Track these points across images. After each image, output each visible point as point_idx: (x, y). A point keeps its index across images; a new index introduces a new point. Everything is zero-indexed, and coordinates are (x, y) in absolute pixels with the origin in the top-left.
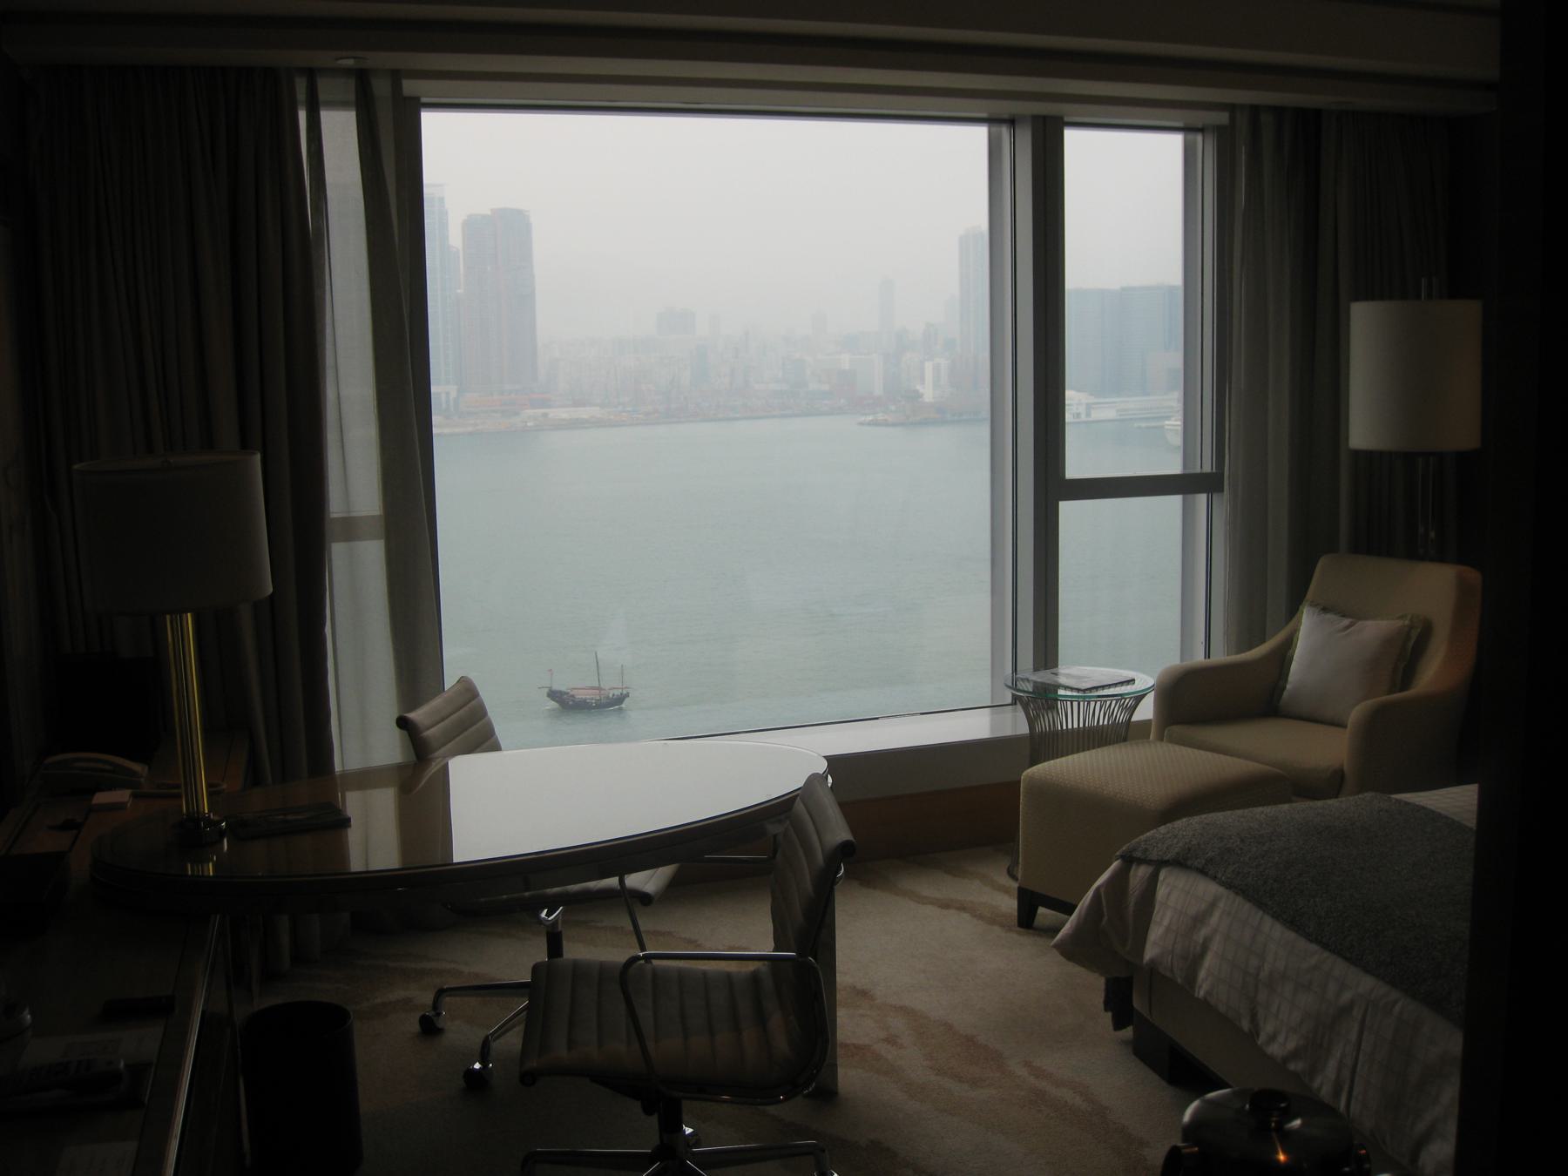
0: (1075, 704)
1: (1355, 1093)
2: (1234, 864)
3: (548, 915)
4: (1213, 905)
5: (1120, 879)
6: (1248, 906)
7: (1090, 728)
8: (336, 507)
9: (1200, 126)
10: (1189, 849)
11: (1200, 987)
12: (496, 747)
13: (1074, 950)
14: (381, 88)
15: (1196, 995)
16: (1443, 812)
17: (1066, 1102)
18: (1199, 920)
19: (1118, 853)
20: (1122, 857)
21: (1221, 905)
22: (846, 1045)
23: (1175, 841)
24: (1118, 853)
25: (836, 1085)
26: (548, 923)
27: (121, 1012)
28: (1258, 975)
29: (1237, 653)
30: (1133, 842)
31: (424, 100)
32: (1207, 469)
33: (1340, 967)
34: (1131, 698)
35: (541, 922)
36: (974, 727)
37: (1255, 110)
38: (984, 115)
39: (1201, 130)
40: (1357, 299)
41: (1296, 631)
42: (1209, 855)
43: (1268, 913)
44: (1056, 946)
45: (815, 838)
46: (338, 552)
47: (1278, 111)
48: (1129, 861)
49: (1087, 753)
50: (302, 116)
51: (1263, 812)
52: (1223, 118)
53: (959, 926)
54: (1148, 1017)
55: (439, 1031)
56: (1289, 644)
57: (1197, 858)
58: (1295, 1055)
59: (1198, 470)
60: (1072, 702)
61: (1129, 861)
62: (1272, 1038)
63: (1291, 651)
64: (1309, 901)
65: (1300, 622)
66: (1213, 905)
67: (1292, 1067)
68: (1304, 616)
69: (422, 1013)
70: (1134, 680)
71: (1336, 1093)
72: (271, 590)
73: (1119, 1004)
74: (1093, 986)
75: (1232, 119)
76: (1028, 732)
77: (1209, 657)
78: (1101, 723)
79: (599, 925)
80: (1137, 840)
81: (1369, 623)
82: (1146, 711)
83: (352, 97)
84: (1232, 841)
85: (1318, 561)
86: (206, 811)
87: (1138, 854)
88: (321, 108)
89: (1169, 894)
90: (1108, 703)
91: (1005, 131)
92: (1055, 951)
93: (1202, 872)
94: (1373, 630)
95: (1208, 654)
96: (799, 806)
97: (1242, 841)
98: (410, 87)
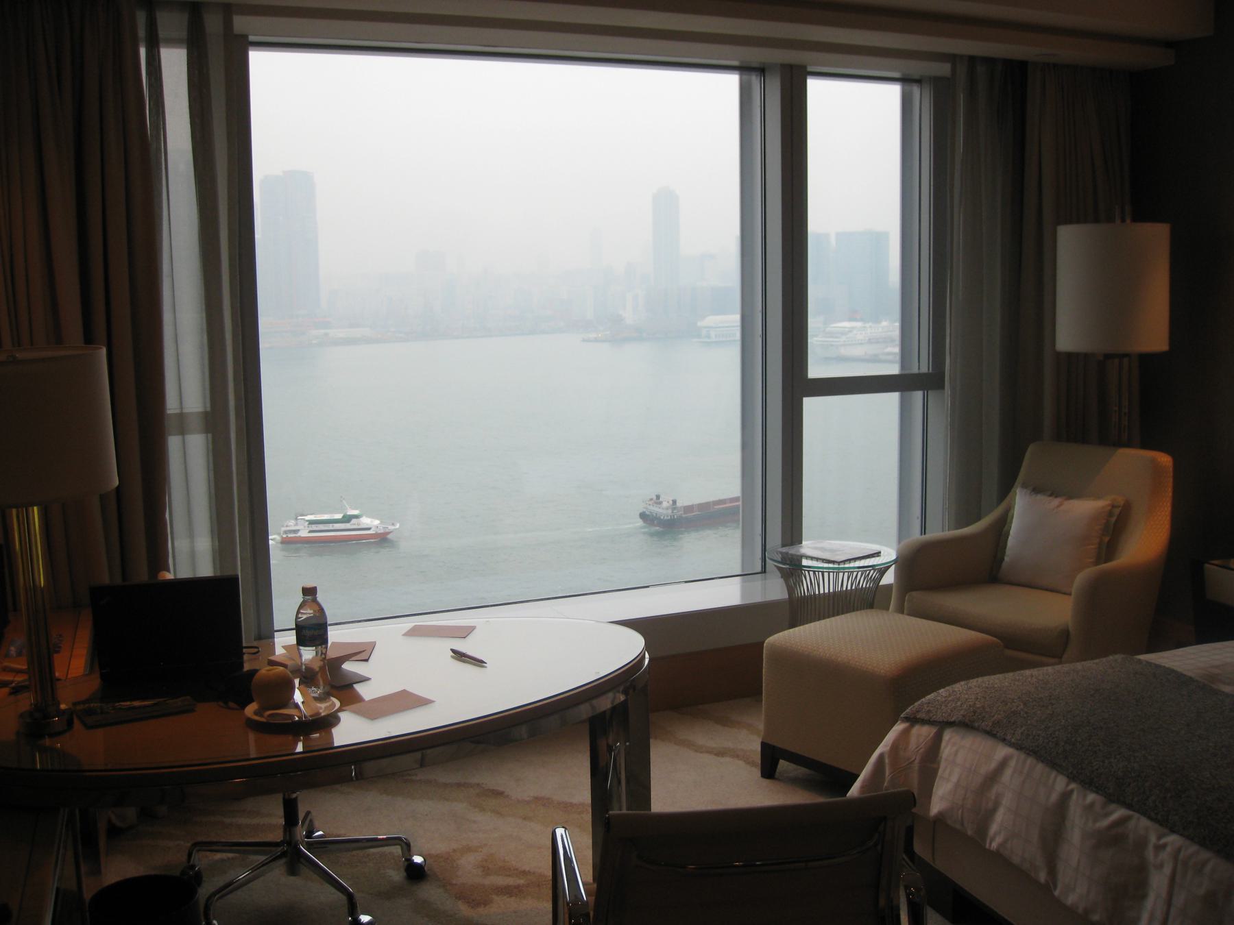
2: (1022, 727)
6: (1040, 766)
7: (834, 592)
8: (172, 405)
9: (917, 77)
10: (975, 712)
11: (992, 840)
14: (213, 23)
15: (987, 846)
19: (902, 716)
21: (1012, 763)
23: (959, 703)
29: (957, 529)
30: (916, 704)
31: (252, 38)
32: (924, 370)
36: (727, 594)
37: (972, 60)
38: (736, 63)
39: (918, 81)
41: (1009, 509)
42: (995, 717)
43: (1062, 773)
46: (173, 443)
47: (989, 61)
50: (143, 52)
51: (1032, 676)
52: (944, 69)
54: (932, 863)
57: (983, 721)
59: (915, 370)
60: (823, 573)
63: (1006, 527)
64: (1103, 762)
66: (1003, 764)
68: (1018, 498)
70: (880, 552)
76: (786, 596)
77: (925, 534)
78: (849, 588)
79: (414, 778)
80: (919, 702)
82: (889, 578)
83: (184, 34)
85: (1028, 447)
88: (161, 44)
89: (956, 753)
90: (855, 574)
91: (755, 80)
93: (990, 734)
94: (1084, 508)
95: (924, 530)
97: (1025, 704)
98: (241, 23)
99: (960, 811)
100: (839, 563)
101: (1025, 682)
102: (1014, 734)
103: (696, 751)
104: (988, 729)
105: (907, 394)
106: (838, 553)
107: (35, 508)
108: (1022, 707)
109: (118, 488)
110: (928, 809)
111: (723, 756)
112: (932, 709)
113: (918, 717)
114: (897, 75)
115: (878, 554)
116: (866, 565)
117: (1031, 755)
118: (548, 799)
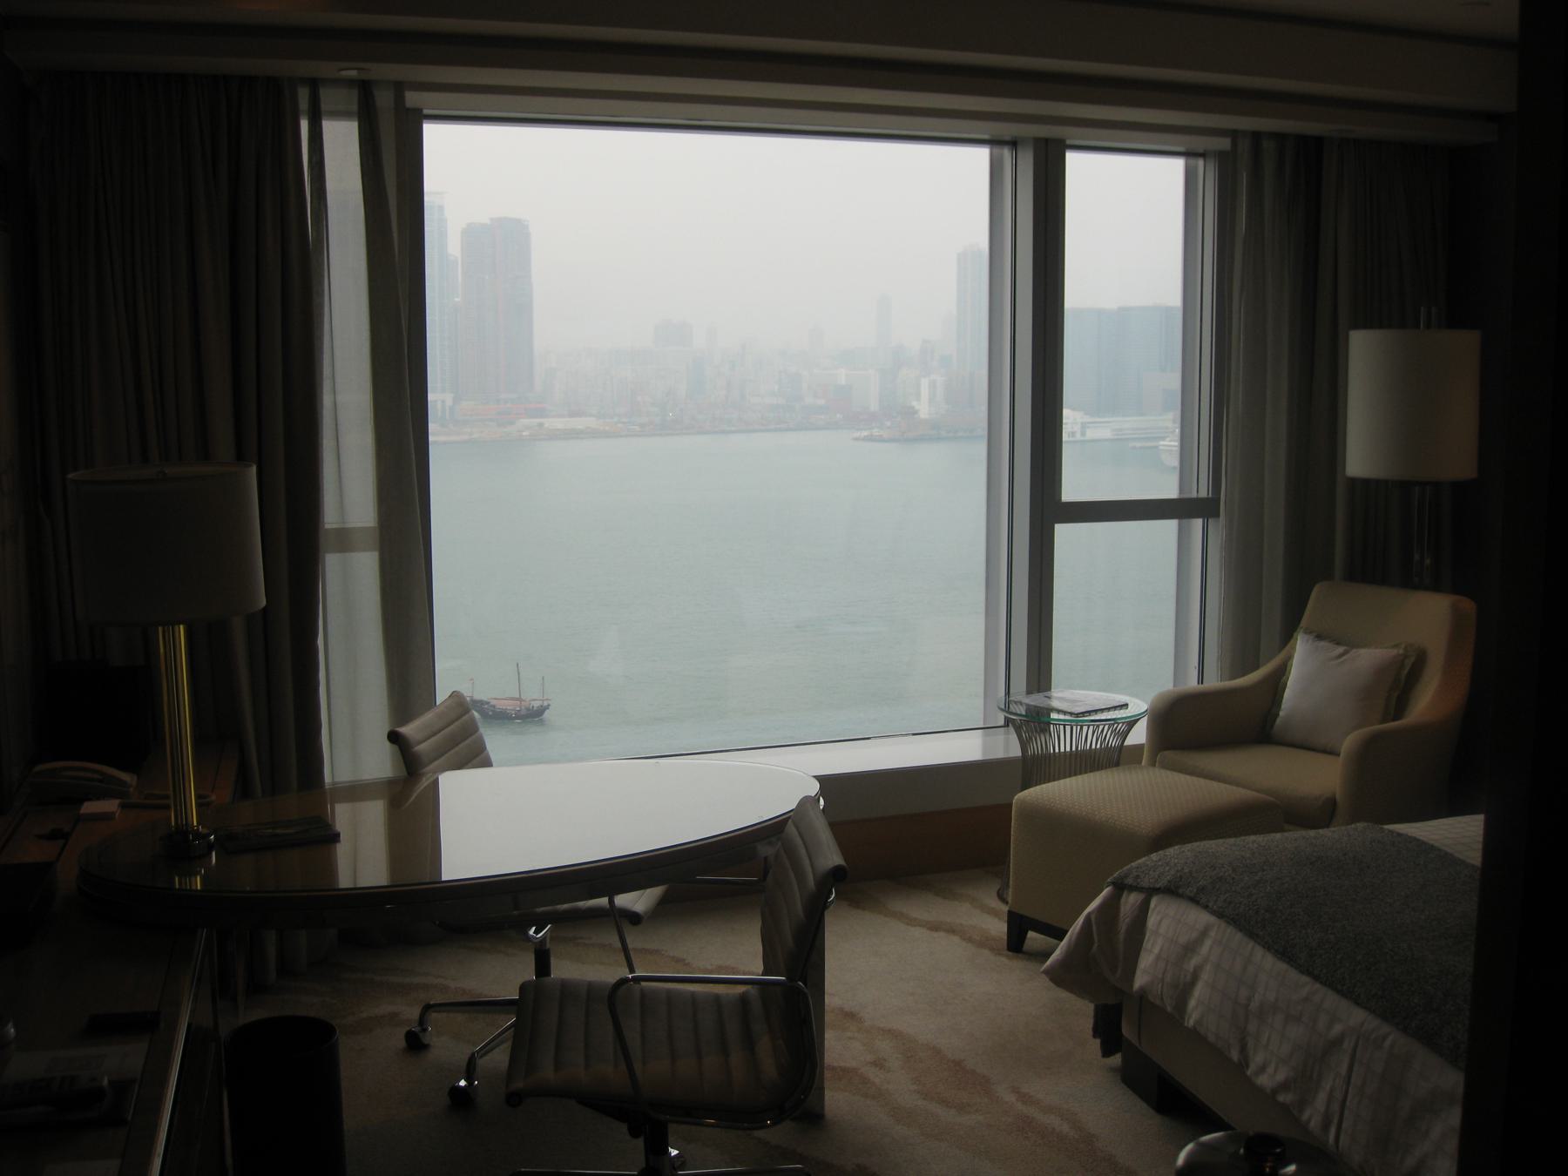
0: (1068, 728)
1: (1344, 1125)
3: (536, 932)
4: (1204, 933)
5: (1111, 906)
6: (1239, 936)
7: (1083, 751)
8: (330, 518)
9: (1201, 151)
10: (1181, 877)
12: (487, 763)
13: (1062, 977)
14: (384, 99)
15: (1186, 1024)
16: (1436, 844)
17: (1054, 1129)
18: (1190, 948)
19: (1109, 880)
20: (1113, 883)
21: (1212, 934)
22: (834, 1068)
23: (1167, 868)
24: (1109, 880)
25: (823, 1107)
26: (537, 941)
27: (105, 1027)
28: (1249, 1005)
30: (1125, 868)
31: (426, 112)
32: (1203, 494)
33: (1330, 999)
34: (1123, 723)
35: (528, 939)
36: (966, 748)
37: (1256, 137)
38: (986, 137)
39: (1203, 155)
40: (1356, 327)
41: (1290, 658)
43: (1259, 944)
44: (1046, 972)
45: (806, 862)
46: (332, 563)
47: (1279, 137)
48: (1120, 887)
49: (1079, 777)
50: (304, 125)
51: (1254, 842)
53: (950, 949)
54: (1137, 1045)
55: (425, 1047)
56: (1281, 672)
58: (1285, 1086)
59: (1194, 495)
60: (1064, 726)
61: (1120, 887)
62: (1262, 1069)
65: (1294, 648)
66: (1204, 933)
67: (1281, 1098)
69: (408, 1029)
71: (1326, 1126)
72: (263, 602)
73: (1108, 1031)
74: (1083, 1012)
75: (1234, 144)
76: (1020, 754)
77: (1202, 683)
78: (1093, 747)
81: (1363, 651)
82: (1139, 735)
83: (355, 107)
84: (1223, 870)
85: (1314, 586)
86: (195, 824)
87: (1129, 881)
88: (324, 118)
90: (1101, 727)
91: (1006, 153)
92: (1044, 976)
93: (1194, 900)
94: (1367, 658)
95: (1201, 680)
96: (791, 829)
97: (1234, 870)
98: (412, 98)
99: (1160, 985)
100: (1077, 715)
101: (1244, 847)
102: (1216, 901)
103: (908, 924)
104: (1192, 895)
105: (1185, 521)
106: (1079, 704)
107: (182, 627)
108: (1230, 872)
109: (265, 609)
110: (1132, 986)
111: (936, 931)
112: (1140, 874)
113: (1126, 882)
114: (1181, 149)
115: (1125, 706)
116: (1109, 717)
117: (1231, 924)
118: (733, 968)
